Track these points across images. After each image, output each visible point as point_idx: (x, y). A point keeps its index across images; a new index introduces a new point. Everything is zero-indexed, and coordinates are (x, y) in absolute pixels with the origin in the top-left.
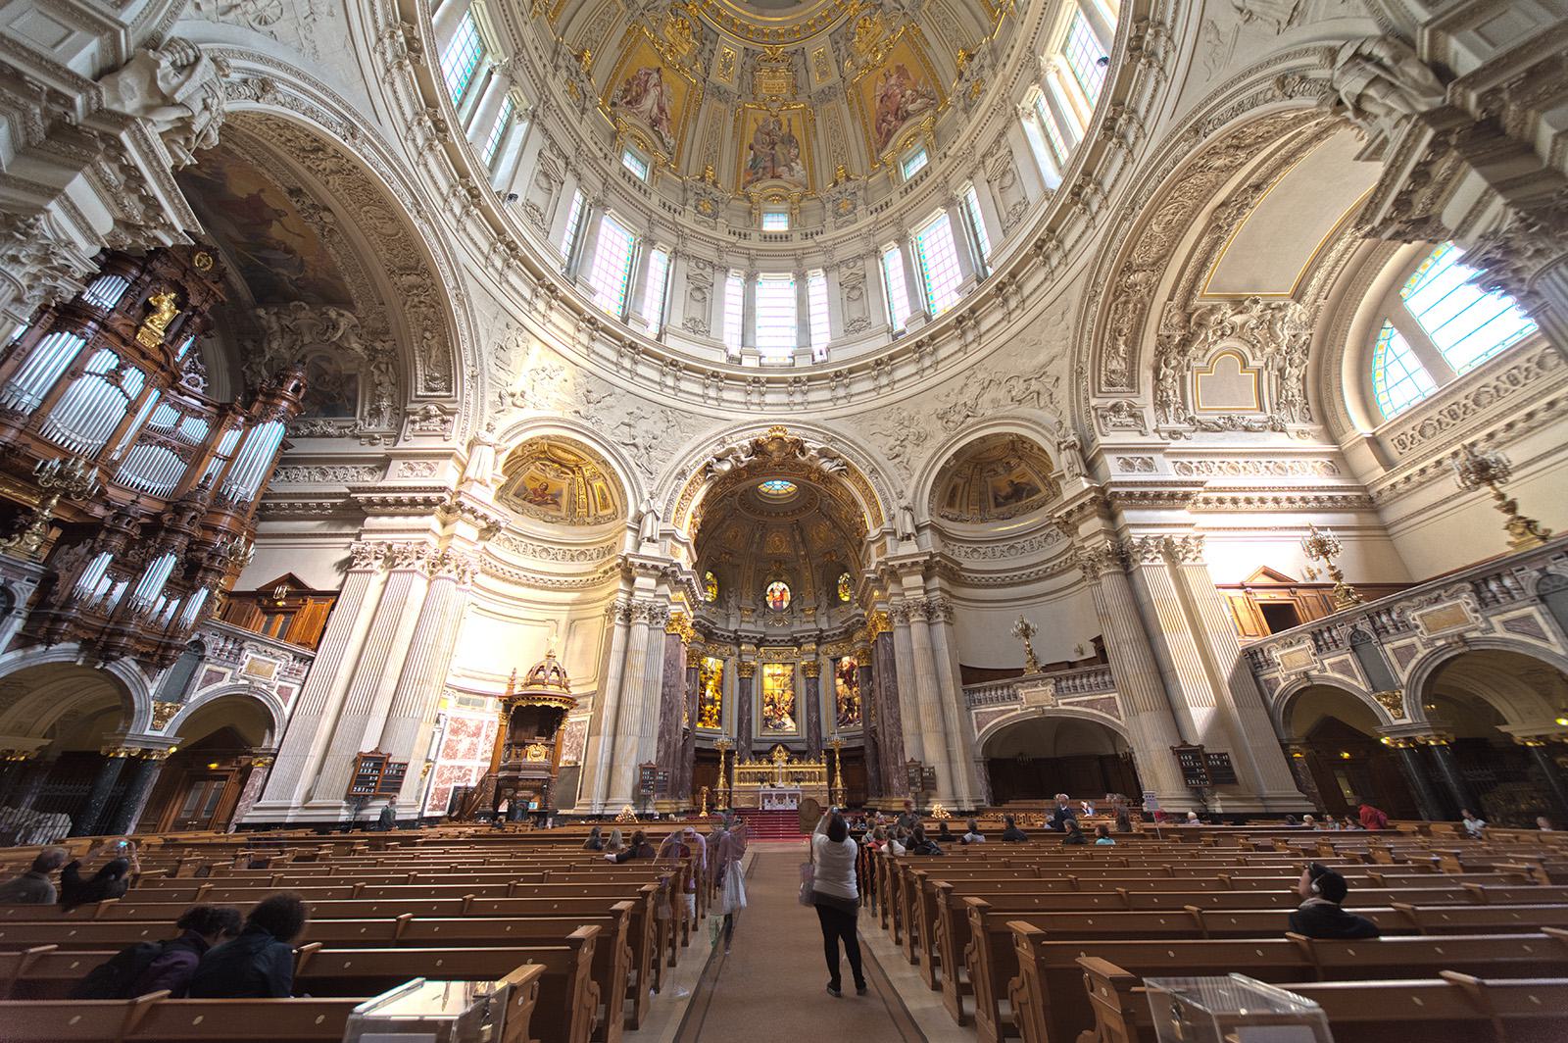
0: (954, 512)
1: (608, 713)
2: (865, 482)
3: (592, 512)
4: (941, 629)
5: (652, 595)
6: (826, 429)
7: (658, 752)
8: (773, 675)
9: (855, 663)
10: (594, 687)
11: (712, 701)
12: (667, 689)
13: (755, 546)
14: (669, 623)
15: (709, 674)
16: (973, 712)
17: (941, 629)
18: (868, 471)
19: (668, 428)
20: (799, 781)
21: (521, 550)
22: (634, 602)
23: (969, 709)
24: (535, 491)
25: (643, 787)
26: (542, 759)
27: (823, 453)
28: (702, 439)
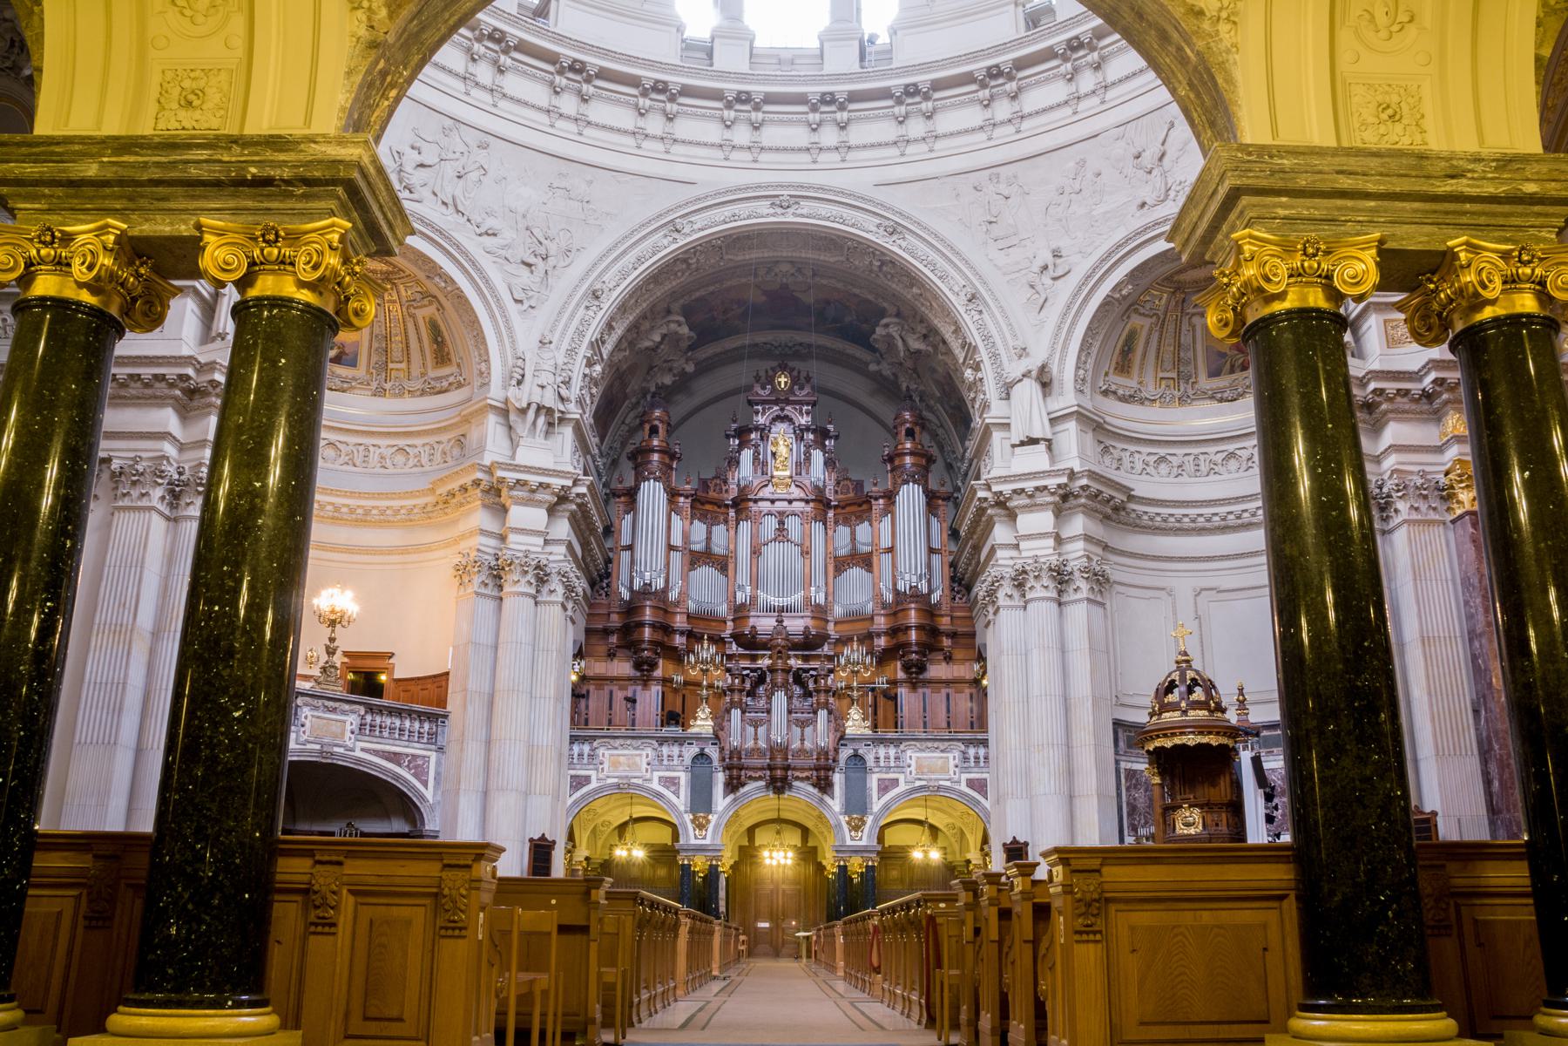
7: (1488, 783)
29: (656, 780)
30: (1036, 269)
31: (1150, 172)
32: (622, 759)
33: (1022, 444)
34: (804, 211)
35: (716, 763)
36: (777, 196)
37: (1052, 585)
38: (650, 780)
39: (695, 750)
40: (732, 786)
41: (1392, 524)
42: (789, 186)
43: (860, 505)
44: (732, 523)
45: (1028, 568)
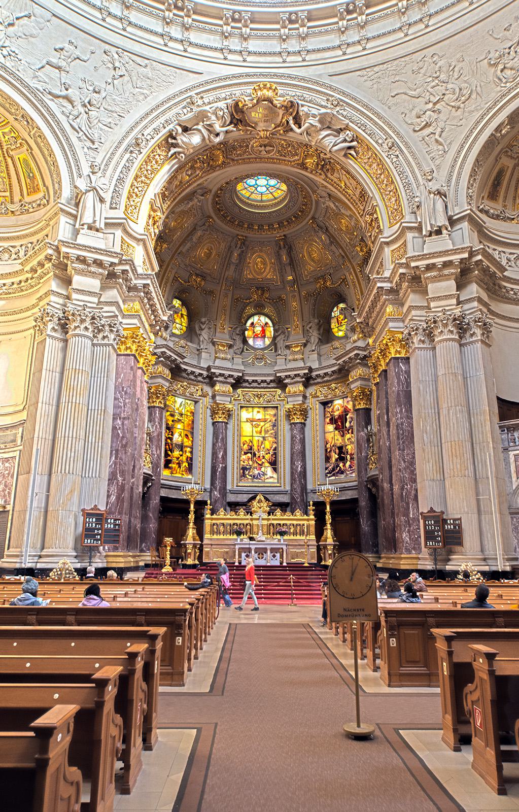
0: (495, 207)
1: (40, 446)
2: (381, 163)
3: (17, 198)
4: (476, 349)
5: (96, 300)
6: (331, 87)
7: (108, 496)
8: (251, 421)
9: (350, 406)
10: (23, 416)
11: (181, 447)
12: (119, 422)
13: (232, 268)
14: (121, 339)
15: (177, 417)
16: (512, 454)
17: (476, 349)
18: (385, 146)
19: (114, 78)
20: (282, 534)
22: (70, 307)
23: (506, 450)
25: (87, 536)
27: (326, 122)
28: (162, 97)
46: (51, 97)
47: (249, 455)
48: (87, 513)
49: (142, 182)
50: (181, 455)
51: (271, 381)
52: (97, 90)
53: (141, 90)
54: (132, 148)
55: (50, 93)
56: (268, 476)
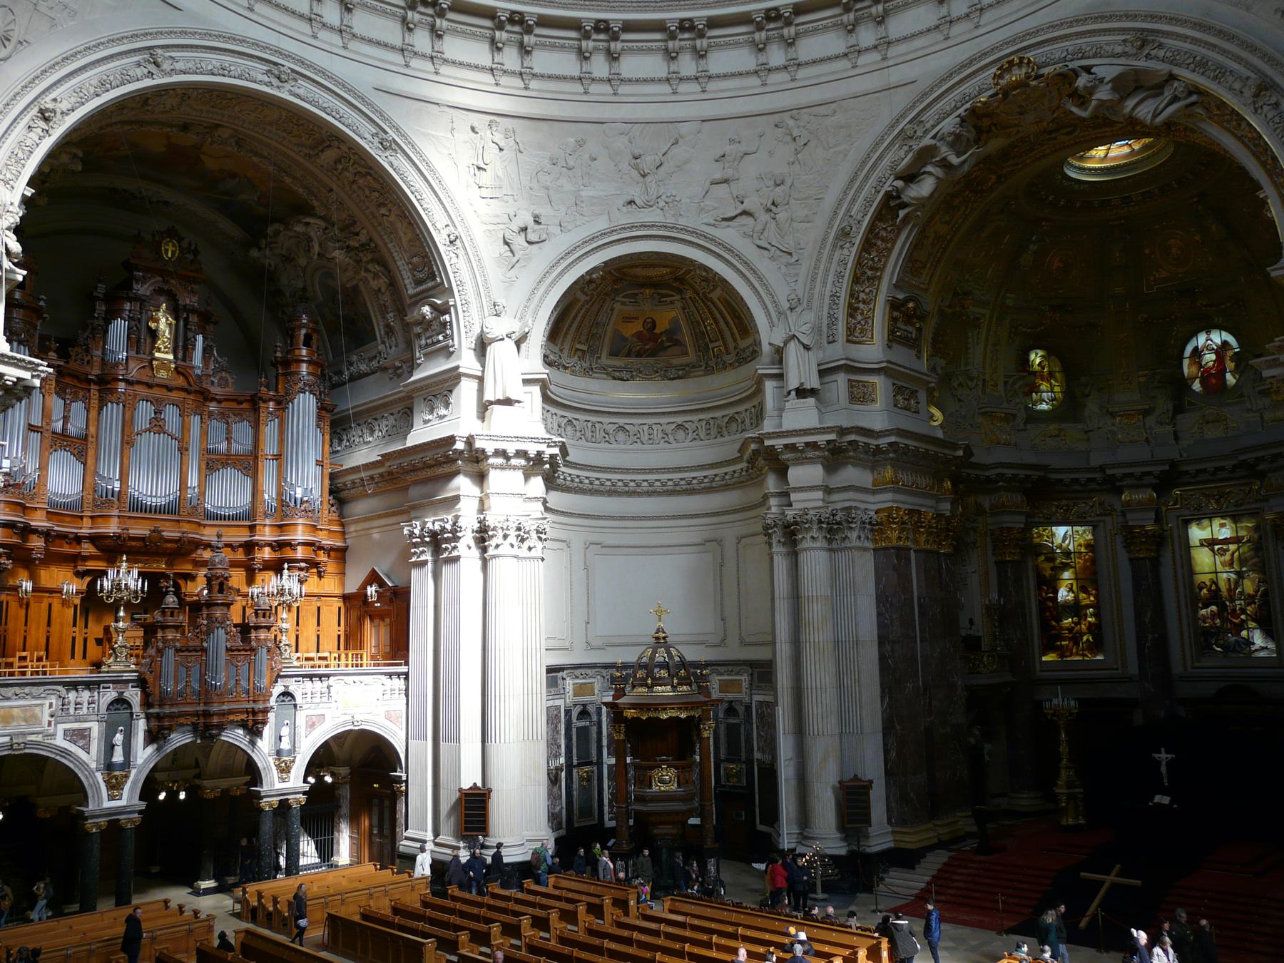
7: (886, 752)
8: (1210, 543)
11: (1075, 609)
19: (797, 152)
21: (645, 438)
24: (639, 335)
26: (674, 787)
28: (866, 142)
29: (60, 734)
30: (516, 229)
31: (644, 176)
32: (15, 711)
33: (499, 402)
34: (301, 92)
35: (136, 708)
36: (276, 64)
37: (515, 544)
38: (53, 735)
39: (110, 694)
40: (153, 737)
41: (834, 545)
42: (288, 56)
43: (240, 403)
44: (95, 402)
45: (497, 525)
46: (726, 223)
47: (1214, 608)
48: (848, 787)
49: (868, 279)
50: (1076, 624)
51: (1235, 467)
52: (778, 182)
53: (837, 149)
54: (840, 244)
55: (724, 219)
56: (1256, 647)
